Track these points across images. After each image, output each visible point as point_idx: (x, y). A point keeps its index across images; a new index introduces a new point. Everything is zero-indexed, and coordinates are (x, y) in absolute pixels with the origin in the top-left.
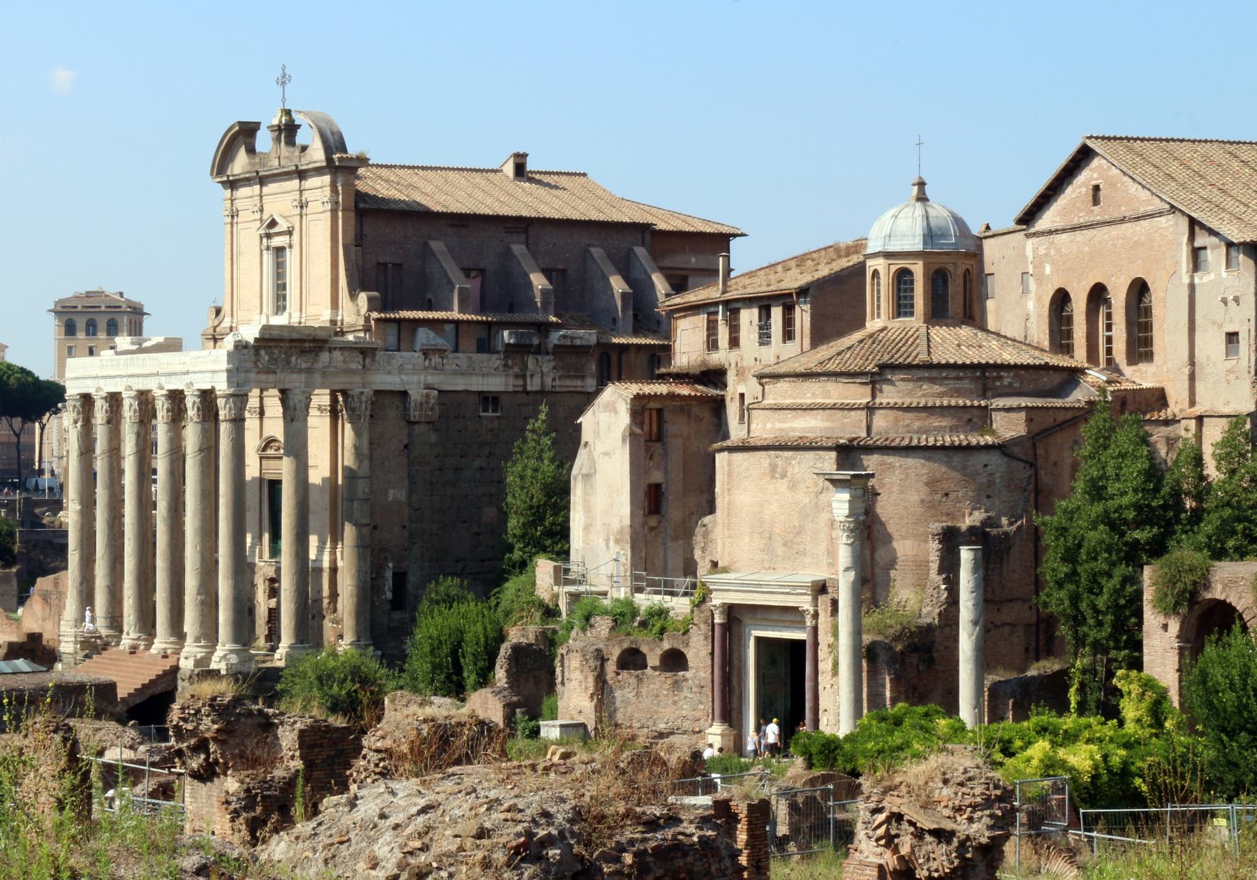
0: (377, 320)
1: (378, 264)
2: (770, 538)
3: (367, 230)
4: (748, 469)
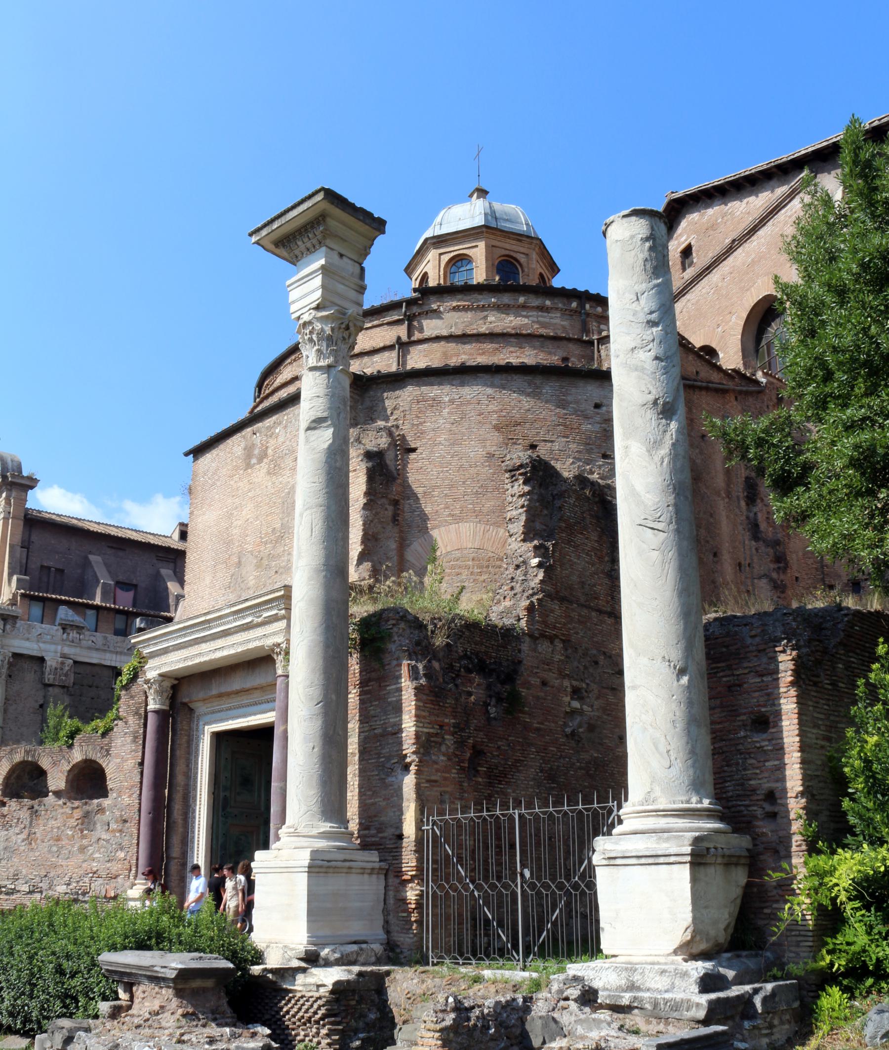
0: (23, 595)
1: (42, 567)
3: (34, 538)
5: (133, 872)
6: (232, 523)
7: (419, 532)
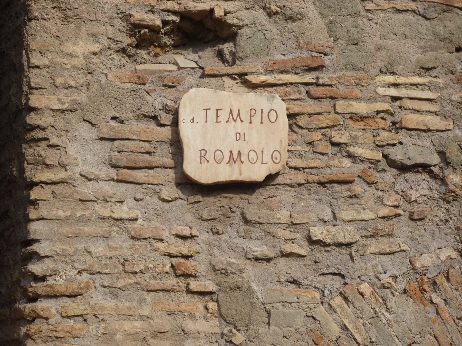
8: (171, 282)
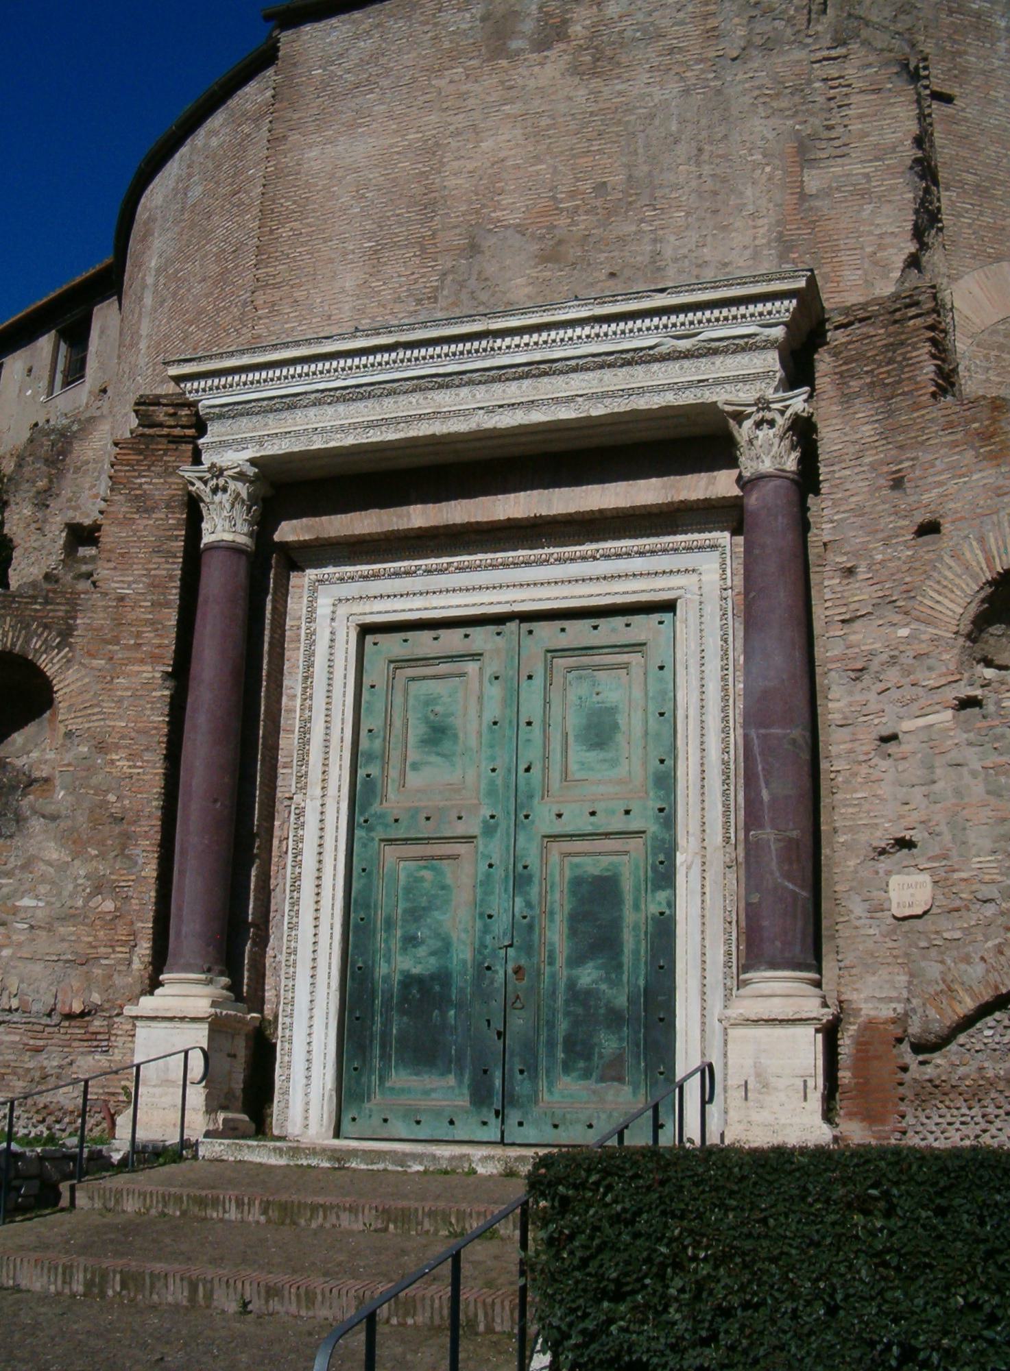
2: (474, 249)
4: (374, 57)
5: (145, 947)
6: (443, 164)
7: (974, 257)
8: (890, 960)
